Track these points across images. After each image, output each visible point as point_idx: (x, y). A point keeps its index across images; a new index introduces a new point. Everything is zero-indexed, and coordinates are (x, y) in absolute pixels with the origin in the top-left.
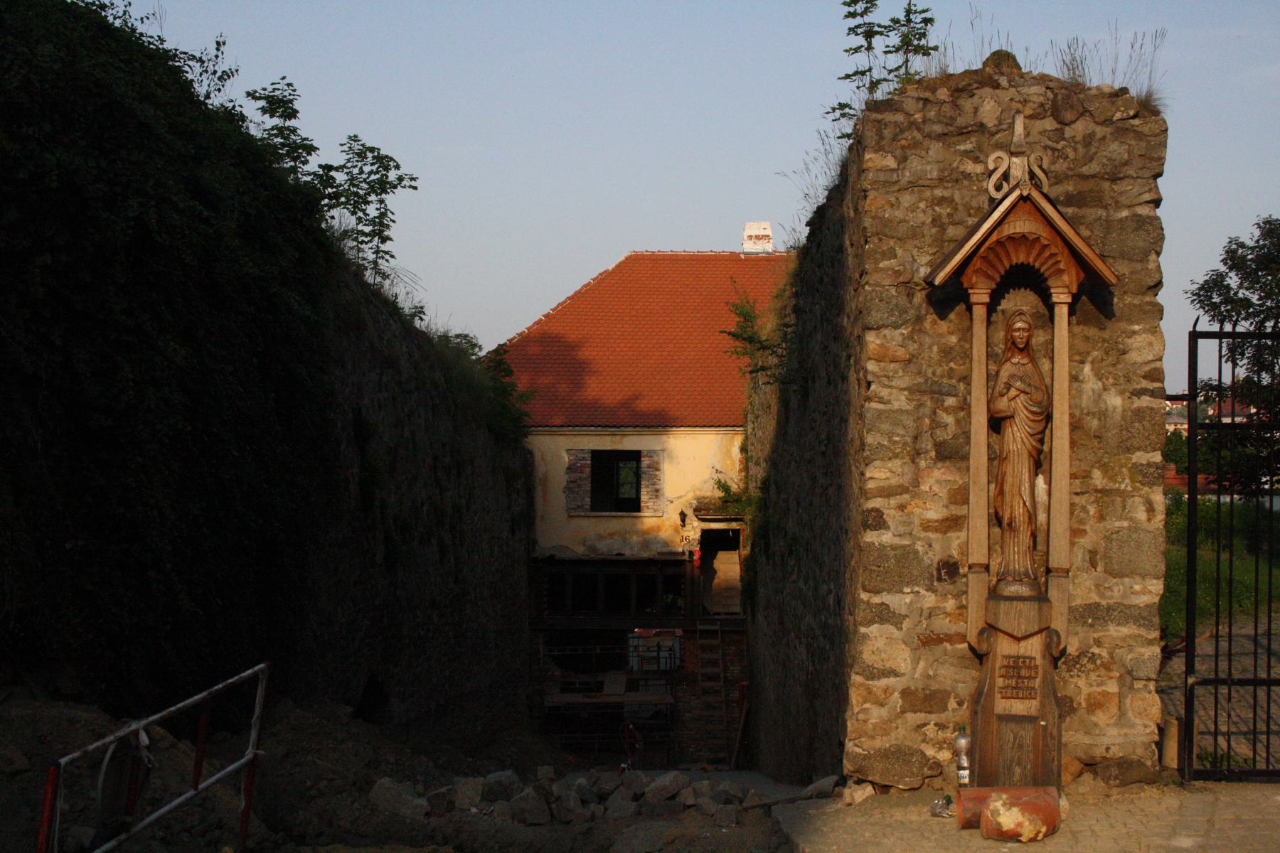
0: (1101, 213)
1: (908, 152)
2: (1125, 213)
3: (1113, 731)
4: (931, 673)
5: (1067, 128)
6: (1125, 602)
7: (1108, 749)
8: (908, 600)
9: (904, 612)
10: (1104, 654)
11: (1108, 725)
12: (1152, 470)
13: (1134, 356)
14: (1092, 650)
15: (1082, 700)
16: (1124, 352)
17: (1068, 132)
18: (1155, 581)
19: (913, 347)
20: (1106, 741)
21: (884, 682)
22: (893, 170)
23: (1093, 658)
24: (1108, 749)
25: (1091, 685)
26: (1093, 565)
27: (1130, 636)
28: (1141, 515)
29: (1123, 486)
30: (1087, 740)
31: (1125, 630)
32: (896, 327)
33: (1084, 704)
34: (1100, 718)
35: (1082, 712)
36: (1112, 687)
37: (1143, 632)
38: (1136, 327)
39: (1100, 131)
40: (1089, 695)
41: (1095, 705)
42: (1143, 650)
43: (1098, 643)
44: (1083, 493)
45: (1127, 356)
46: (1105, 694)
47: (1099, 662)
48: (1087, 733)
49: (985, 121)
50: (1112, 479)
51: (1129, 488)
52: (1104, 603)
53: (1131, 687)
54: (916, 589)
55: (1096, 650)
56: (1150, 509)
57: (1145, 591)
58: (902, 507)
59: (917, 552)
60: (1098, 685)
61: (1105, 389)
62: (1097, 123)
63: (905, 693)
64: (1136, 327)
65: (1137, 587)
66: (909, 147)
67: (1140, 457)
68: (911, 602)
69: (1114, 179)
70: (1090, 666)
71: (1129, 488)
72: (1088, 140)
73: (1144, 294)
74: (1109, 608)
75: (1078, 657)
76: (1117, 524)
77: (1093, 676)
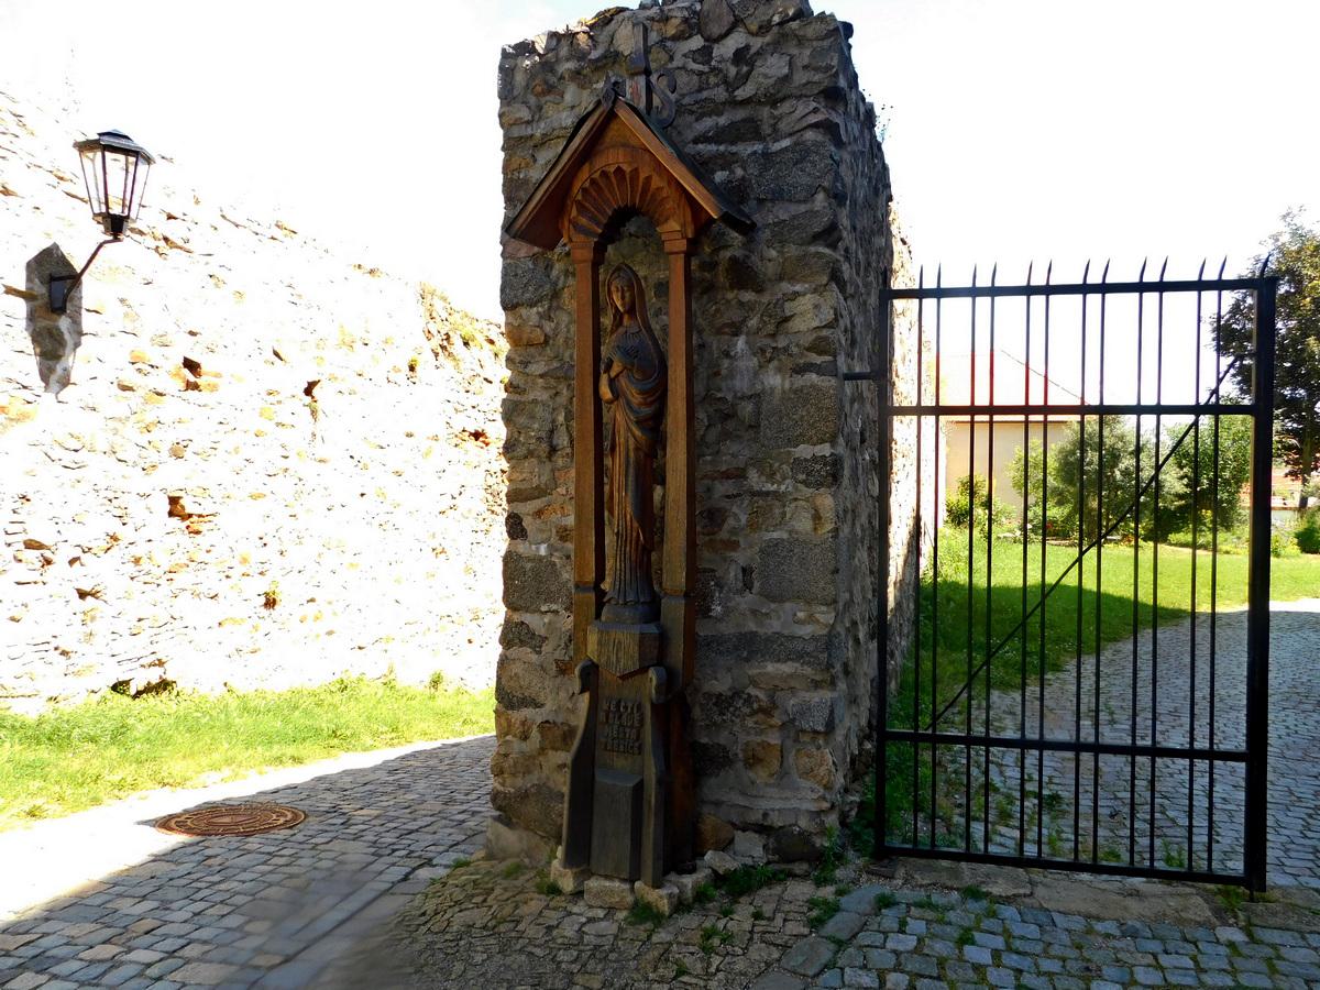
0: (758, 147)
1: (543, 100)
2: (786, 143)
3: (773, 791)
4: (570, 706)
5: (716, 46)
6: (786, 632)
7: (765, 815)
8: (546, 620)
9: (543, 632)
10: (762, 695)
11: (767, 785)
12: (818, 467)
13: (798, 324)
14: (747, 691)
15: (738, 750)
16: (787, 319)
17: (718, 50)
18: (824, 608)
19: (548, 327)
20: (764, 804)
21: (527, 712)
22: (528, 122)
23: (749, 700)
24: (765, 815)
25: (748, 734)
26: (748, 586)
27: (791, 676)
28: (804, 524)
29: (783, 488)
30: (741, 801)
31: (787, 668)
32: (532, 305)
33: (741, 756)
34: (761, 775)
35: (740, 765)
36: (774, 739)
37: (808, 670)
38: (798, 288)
39: (756, 43)
40: (747, 744)
41: (753, 761)
42: (807, 695)
43: (754, 683)
44: (735, 496)
45: (790, 324)
46: (766, 746)
47: (755, 706)
48: (744, 794)
49: (621, 49)
50: (771, 477)
51: (790, 489)
52: (761, 631)
53: (796, 740)
54: (554, 607)
55: (753, 691)
56: (817, 517)
57: (811, 619)
58: (539, 513)
59: (554, 564)
60: (756, 734)
61: (761, 367)
62: (752, 34)
63: (545, 726)
64: (798, 288)
65: (801, 615)
66: (544, 93)
67: (804, 451)
68: (550, 623)
69: (774, 101)
70: (746, 710)
71: (790, 489)
72: (740, 56)
73: (809, 244)
74: (769, 640)
75: (731, 698)
76: (775, 535)
77: (750, 723)
